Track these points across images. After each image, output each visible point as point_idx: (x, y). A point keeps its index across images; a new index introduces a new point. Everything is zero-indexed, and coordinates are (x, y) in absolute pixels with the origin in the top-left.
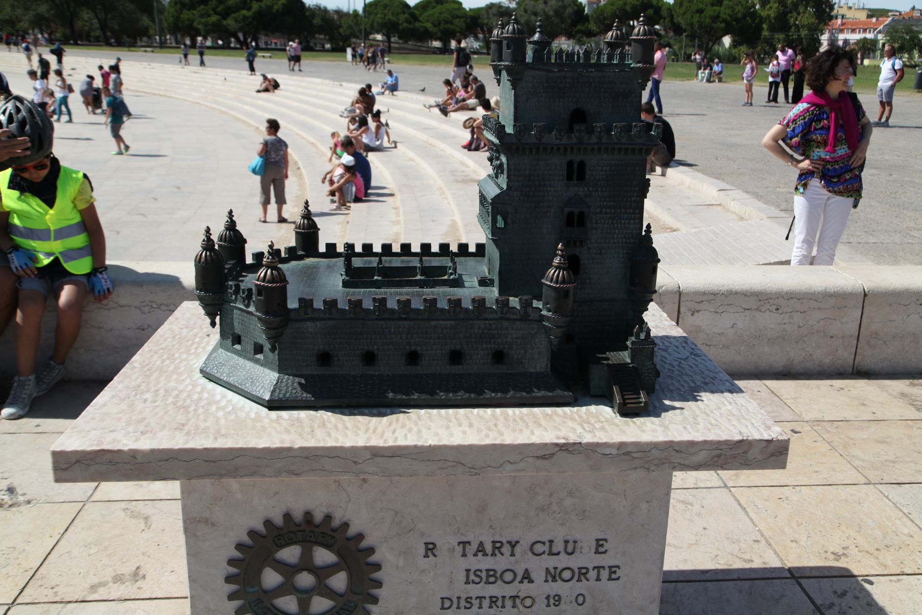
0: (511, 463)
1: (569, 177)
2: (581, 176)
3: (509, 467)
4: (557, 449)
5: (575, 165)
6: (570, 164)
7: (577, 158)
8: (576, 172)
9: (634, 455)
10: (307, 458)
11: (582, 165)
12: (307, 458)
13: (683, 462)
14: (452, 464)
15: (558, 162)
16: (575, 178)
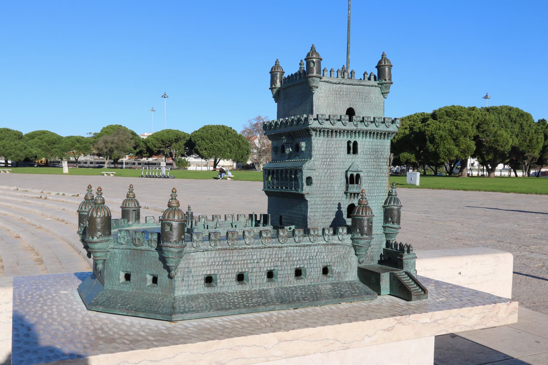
0: (369, 336)
1: (349, 152)
2: (355, 152)
3: (367, 340)
4: (396, 322)
5: (351, 145)
6: (349, 142)
7: (352, 140)
8: (353, 148)
9: (440, 322)
10: (231, 349)
11: (355, 143)
12: (231, 349)
13: (466, 324)
14: (331, 342)
15: (342, 142)
16: (352, 151)
